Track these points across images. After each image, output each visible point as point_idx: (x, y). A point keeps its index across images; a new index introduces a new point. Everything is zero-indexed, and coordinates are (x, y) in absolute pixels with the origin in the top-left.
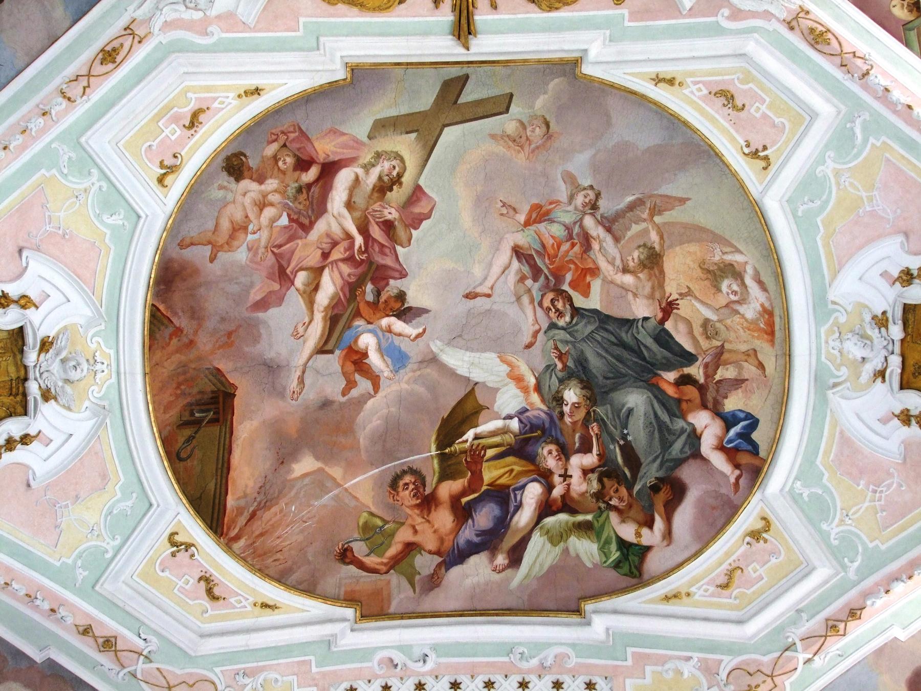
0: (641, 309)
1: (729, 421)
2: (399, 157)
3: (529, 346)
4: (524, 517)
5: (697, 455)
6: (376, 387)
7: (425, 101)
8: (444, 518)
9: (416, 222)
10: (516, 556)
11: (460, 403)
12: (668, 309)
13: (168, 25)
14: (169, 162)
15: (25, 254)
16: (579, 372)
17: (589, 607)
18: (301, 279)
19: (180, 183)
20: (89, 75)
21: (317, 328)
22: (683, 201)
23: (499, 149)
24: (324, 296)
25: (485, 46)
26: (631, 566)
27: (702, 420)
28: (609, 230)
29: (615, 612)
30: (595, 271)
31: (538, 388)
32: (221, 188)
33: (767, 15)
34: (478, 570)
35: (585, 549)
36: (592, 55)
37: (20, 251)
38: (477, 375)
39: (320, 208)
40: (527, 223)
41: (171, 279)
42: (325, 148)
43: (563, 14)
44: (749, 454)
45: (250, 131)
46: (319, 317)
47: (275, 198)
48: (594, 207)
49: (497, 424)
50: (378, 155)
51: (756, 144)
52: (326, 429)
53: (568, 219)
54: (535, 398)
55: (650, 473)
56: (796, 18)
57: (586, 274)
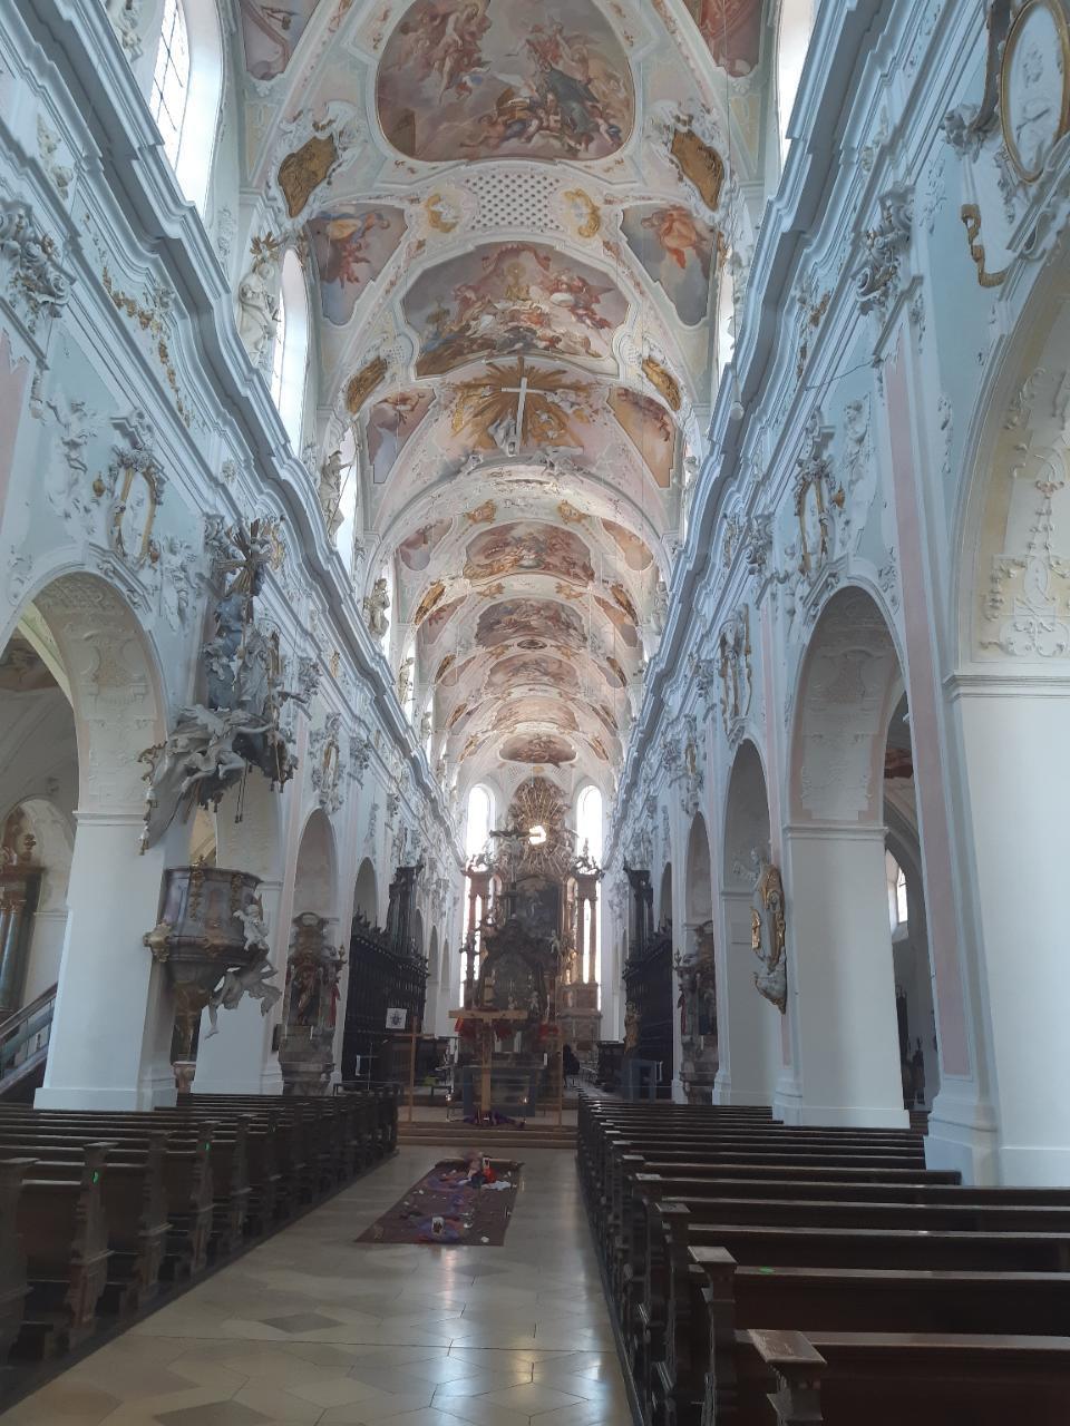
0: (578, 77)
1: (611, 126)
2: (475, 5)
3: (534, 75)
4: (532, 129)
5: (598, 130)
6: (471, 92)
8: (500, 128)
9: (485, 30)
10: (529, 139)
11: (506, 92)
12: (590, 81)
14: (376, 37)
16: (553, 90)
17: (557, 160)
18: (436, 65)
19: (382, 46)
21: (445, 81)
22: (597, 43)
24: (447, 68)
26: (573, 154)
27: (601, 121)
28: (567, 42)
29: (567, 164)
30: (561, 56)
31: (537, 91)
34: (513, 143)
35: (556, 143)
38: (513, 83)
39: (443, 33)
40: (532, 32)
41: (384, 84)
42: (442, 9)
44: (617, 139)
45: (408, 13)
46: (445, 76)
48: (560, 31)
49: (521, 99)
51: (629, 34)
52: (452, 112)
53: (550, 33)
54: (536, 94)
55: (579, 130)
57: (556, 57)
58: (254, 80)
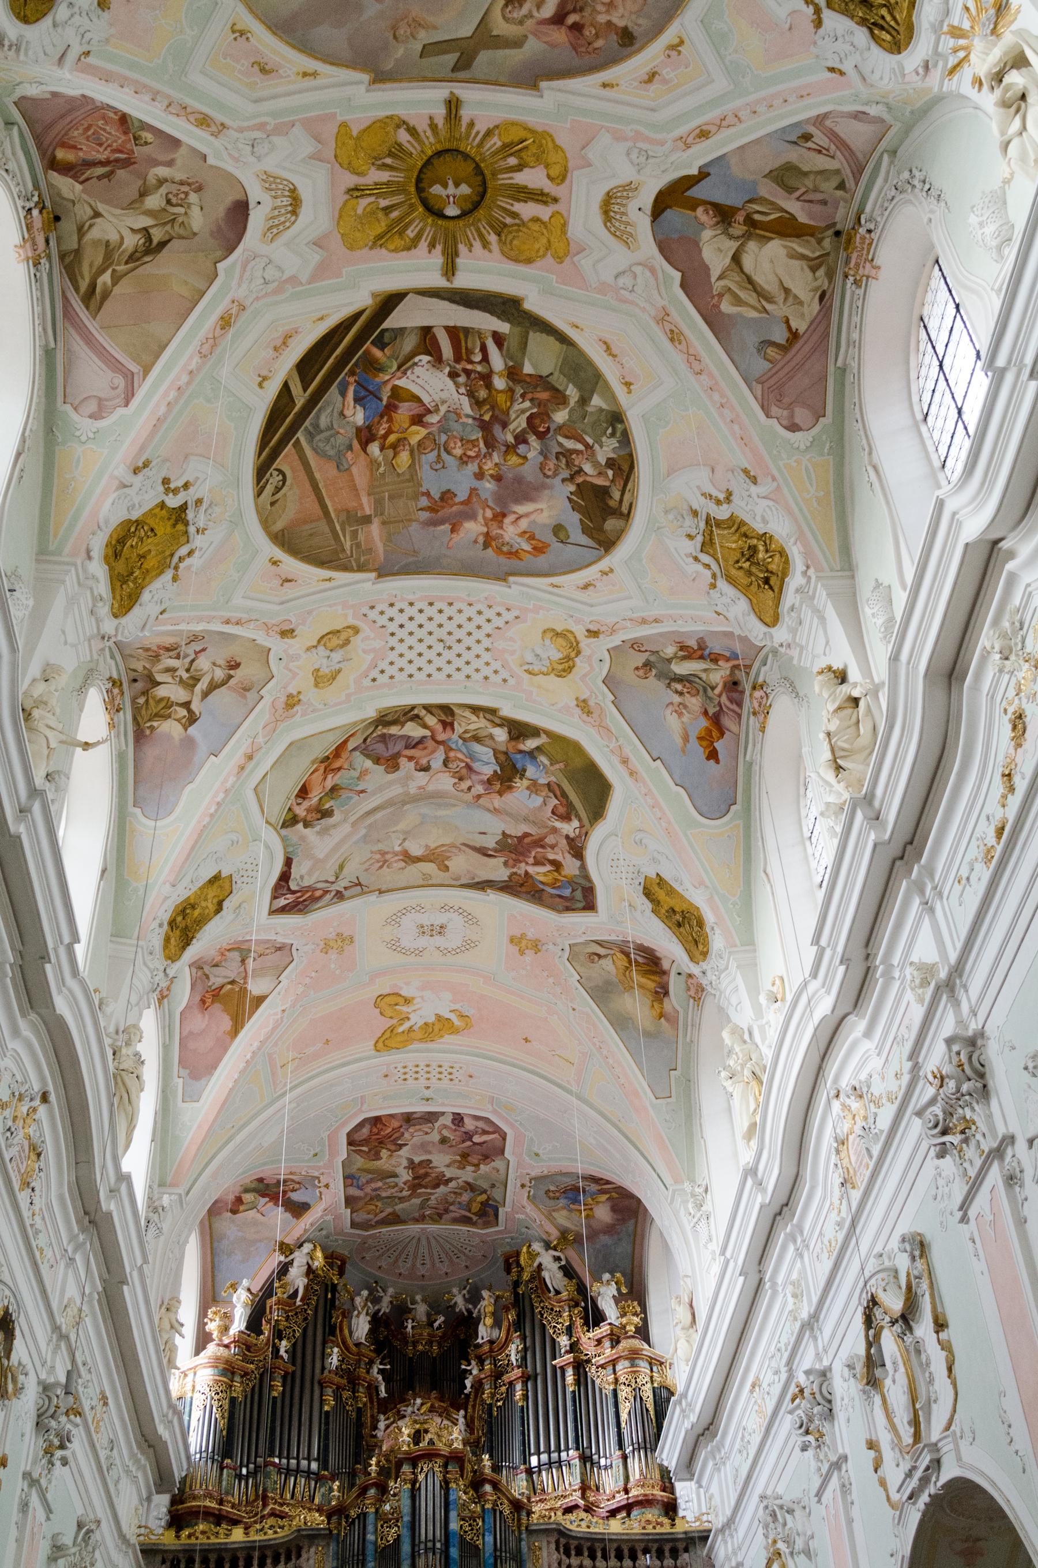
7: (484, 57)
13: (662, 143)
14: (674, 53)
15: (787, 26)
20: (720, 127)
23: (431, 19)
25: (439, 93)
32: (639, 25)
33: (241, 130)
36: (362, 88)
37: (790, 29)
42: (560, 35)
43: (382, 114)
45: (613, 60)
47: (600, 8)
50: (521, 23)
51: (242, 40)
56: (220, 132)
58: (886, 116)
